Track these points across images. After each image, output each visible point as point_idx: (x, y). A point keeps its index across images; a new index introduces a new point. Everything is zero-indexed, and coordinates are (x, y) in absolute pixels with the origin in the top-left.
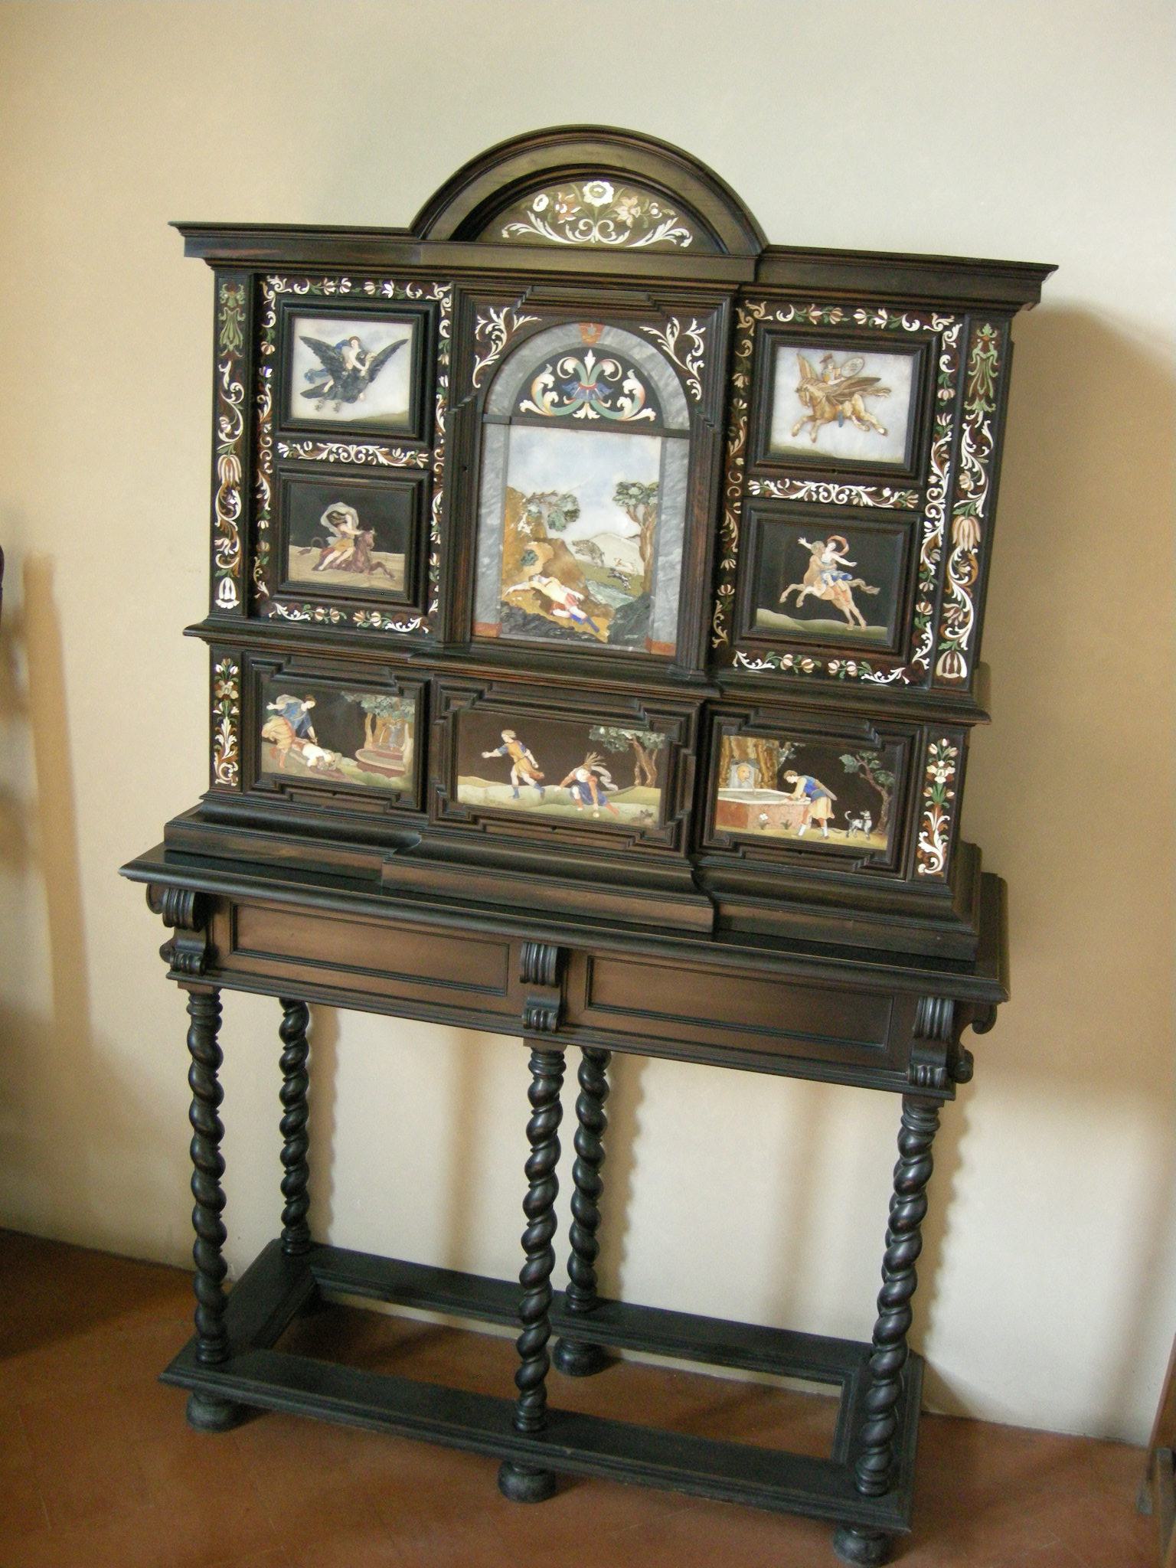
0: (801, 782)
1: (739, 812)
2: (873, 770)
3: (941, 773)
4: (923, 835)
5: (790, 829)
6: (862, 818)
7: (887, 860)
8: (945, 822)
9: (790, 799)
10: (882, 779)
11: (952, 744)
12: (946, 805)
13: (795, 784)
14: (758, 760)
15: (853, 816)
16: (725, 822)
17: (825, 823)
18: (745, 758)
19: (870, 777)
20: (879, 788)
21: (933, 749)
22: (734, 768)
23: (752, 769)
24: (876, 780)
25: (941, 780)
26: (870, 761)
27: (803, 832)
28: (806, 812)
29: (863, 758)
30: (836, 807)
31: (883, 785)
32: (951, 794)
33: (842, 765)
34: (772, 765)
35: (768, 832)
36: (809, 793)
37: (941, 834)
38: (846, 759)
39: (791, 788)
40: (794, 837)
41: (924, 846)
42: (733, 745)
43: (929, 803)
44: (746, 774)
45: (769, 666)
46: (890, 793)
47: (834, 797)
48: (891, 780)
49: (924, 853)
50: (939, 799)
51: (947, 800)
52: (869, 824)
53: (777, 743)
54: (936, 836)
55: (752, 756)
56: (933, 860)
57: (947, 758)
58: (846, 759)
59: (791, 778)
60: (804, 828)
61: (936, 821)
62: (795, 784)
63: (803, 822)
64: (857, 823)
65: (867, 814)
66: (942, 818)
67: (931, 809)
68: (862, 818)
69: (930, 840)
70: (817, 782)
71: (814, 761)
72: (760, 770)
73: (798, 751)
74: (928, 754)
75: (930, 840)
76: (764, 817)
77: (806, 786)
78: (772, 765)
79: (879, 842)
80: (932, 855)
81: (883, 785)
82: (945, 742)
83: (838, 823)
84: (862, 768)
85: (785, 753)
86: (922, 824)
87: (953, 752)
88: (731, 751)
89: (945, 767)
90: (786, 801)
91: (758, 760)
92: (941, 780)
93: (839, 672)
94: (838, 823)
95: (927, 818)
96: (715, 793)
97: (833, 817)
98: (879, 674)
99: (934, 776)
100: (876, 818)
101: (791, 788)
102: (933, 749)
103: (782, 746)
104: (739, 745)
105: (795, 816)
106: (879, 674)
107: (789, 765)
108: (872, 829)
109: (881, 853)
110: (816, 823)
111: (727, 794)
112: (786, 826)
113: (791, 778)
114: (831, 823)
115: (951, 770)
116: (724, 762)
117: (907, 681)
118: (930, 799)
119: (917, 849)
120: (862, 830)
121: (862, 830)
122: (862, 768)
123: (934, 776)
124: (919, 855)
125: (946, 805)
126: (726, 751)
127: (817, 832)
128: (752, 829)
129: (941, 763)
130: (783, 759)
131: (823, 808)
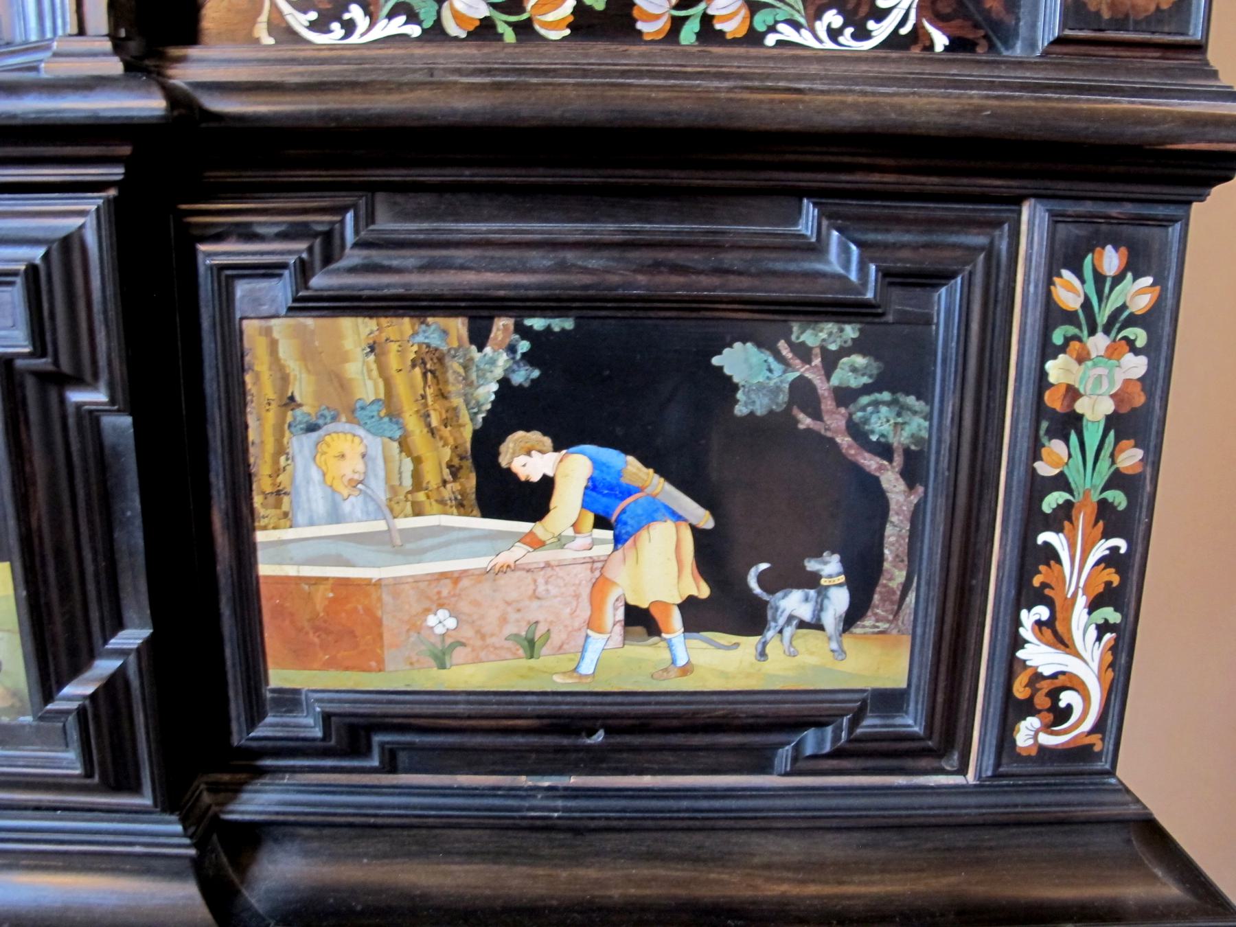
0: (571, 470)
1: (349, 616)
2: (845, 396)
3: (1095, 378)
4: (1042, 612)
5: (546, 659)
6: (812, 581)
7: (911, 722)
8: (1111, 559)
9: (536, 543)
10: (881, 424)
11: (1135, 266)
12: (1118, 498)
13: (547, 484)
14: (390, 407)
15: (776, 582)
16: (301, 657)
17: (676, 619)
18: (341, 406)
19: (834, 422)
20: (870, 463)
21: (1069, 292)
22: (300, 445)
23: (375, 445)
24: (857, 431)
25: (1095, 409)
26: (830, 362)
27: (602, 662)
28: (600, 585)
29: (804, 353)
30: (711, 553)
31: (884, 450)
32: (1131, 458)
33: (727, 387)
34: (451, 419)
35: (469, 675)
36: (608, 513)
37: (1093, 607)
38: (739, 361)
39: (531, 501)
40: (561, 683)
41: (1039, 656)
42: (286, 351)
43: (1051, 502)
44: (353, 466)
45: (398, 26)
46: (912, 473)
47: (706, 520)
48: (917, 425)
49: (1037, 677)
50: (1089, 483)
51: (1117, 480)
52: (840, 600)
53: (458, 326)
54: (1080, 621)
55: (368, 389)
56: (1066, 698)
57: (1120, 319)
58: (739, 361)
59: (529, 458)
60: (597, 643)
61: (1077, 558)
62: (547, 484)
63: (594, 624)
64: (794, 603)
65: (830, 567)
66: (1101, 549)
67: (1061, 519)
68: (812, 581)
69: (1055, 633)
70: (632, 468)
71: (616, 382)
72: (404, 445)
73: (542, 349)
74: (1053, 315)
75: (1055, 633)
76: (441, 622)
77: (593, 487)
78: (451, 419)
79: (878, 661)
80: (1063, 682)
81: (884, 450)
82: (1111, 260)
83: (728, 606)
84: (803, 394)
85: (498, 362)
86: (1030, 577)
87: (1138, 294)
88: (284, 379)
89: (1112, 353)
90: (519, 551)
91: (390, 407)
92: (1095, 409)
93: (677, 24)
94: (728, 606)
95: (1050, 554)
96: (245, 553)
97: (704, 591)
98: (833, 18)
99: (1072, 393)
100: (863, 579)
101: (531, 501)
102: (1069, 292)
103: (479, 338)
104: (307, 354)
105: (559, 607)
106: (833, 18)
107: (513, 410)
108: (851, 619)
109: (888, 701)
110: (640, 620)
111: (287, 551)
112: (531, 646)
113: (529, 458)
114: (696, 616)
115: (1136, 366)
116: (260, 427)
117: (940, 41)
118: (1061, 482)
119: (1012, 666)
120: (818, 626)
121: (818, 626)
122: (803, 394)
123: (1072, 393)
124: (1020, 690)
125: (1118, 498)
126: (260, 385)
127: (648, 652)
128: (400, 673)
129: (1098, 343)
130: (487, 392)
131: (662, 566)
